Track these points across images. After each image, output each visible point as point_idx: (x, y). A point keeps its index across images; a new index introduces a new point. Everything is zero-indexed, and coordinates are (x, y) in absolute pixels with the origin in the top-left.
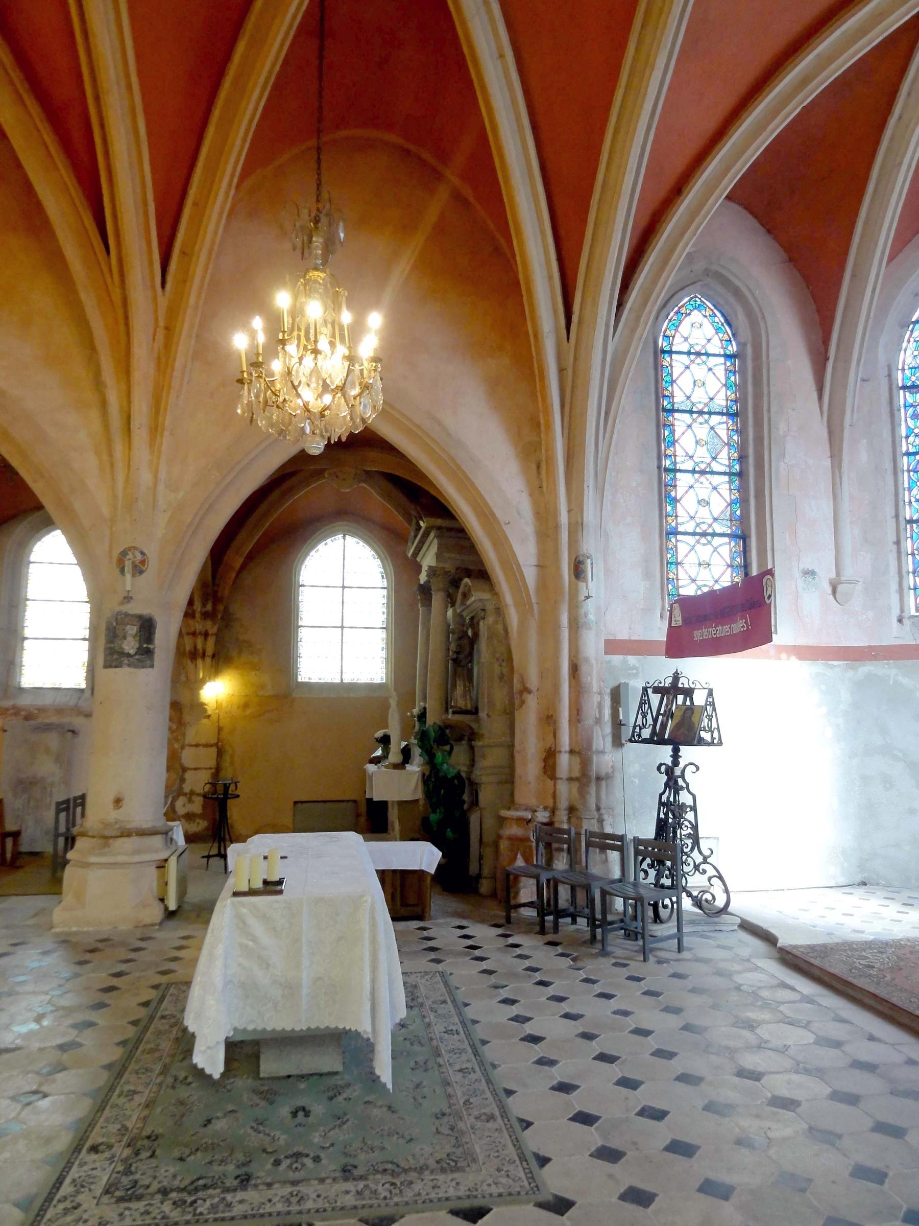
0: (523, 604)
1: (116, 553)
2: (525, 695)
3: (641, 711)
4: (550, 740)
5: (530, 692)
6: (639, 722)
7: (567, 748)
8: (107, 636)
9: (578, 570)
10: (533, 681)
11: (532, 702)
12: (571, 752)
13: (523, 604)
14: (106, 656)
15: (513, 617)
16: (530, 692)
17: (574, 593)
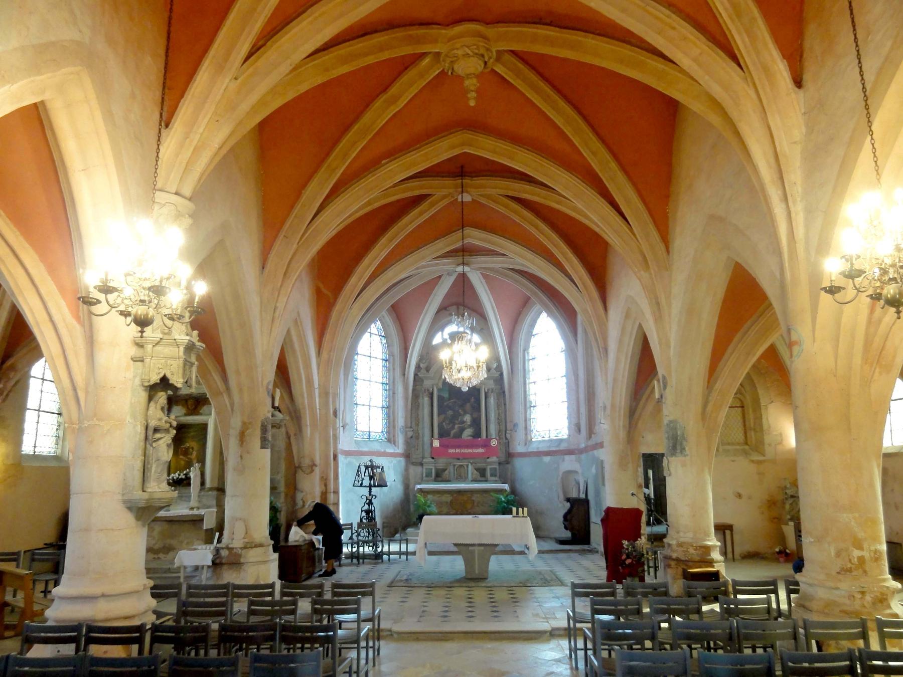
0: (314, 425)
1: (265, 383)
2: (314, 468)
3: (367, 474)
4: (323, 487)
5: (316, 466)
6: (357, 479)
7: (332, 491)
8: (262, 430)
9: (335, 414)
10: (318, 461)
11: (317, 470)
12: (334, 492)
13: (314, 425)
14: (262, 442)
15: (308, 431)
16: (316, 466)
17: (335, 423)
